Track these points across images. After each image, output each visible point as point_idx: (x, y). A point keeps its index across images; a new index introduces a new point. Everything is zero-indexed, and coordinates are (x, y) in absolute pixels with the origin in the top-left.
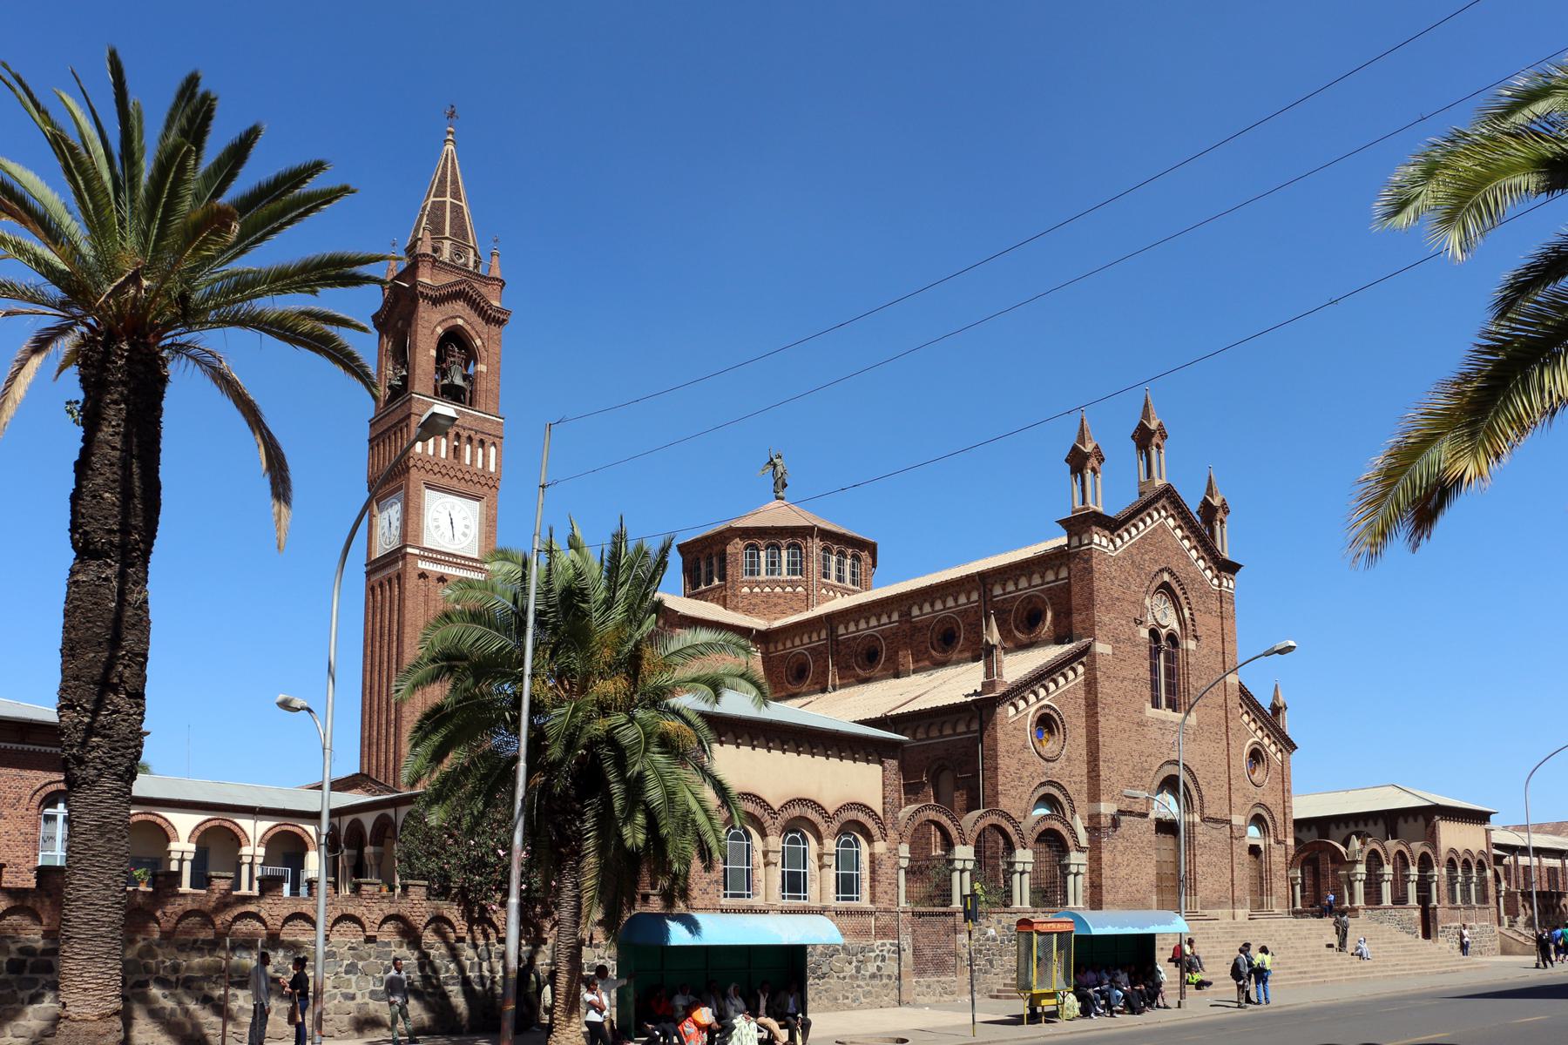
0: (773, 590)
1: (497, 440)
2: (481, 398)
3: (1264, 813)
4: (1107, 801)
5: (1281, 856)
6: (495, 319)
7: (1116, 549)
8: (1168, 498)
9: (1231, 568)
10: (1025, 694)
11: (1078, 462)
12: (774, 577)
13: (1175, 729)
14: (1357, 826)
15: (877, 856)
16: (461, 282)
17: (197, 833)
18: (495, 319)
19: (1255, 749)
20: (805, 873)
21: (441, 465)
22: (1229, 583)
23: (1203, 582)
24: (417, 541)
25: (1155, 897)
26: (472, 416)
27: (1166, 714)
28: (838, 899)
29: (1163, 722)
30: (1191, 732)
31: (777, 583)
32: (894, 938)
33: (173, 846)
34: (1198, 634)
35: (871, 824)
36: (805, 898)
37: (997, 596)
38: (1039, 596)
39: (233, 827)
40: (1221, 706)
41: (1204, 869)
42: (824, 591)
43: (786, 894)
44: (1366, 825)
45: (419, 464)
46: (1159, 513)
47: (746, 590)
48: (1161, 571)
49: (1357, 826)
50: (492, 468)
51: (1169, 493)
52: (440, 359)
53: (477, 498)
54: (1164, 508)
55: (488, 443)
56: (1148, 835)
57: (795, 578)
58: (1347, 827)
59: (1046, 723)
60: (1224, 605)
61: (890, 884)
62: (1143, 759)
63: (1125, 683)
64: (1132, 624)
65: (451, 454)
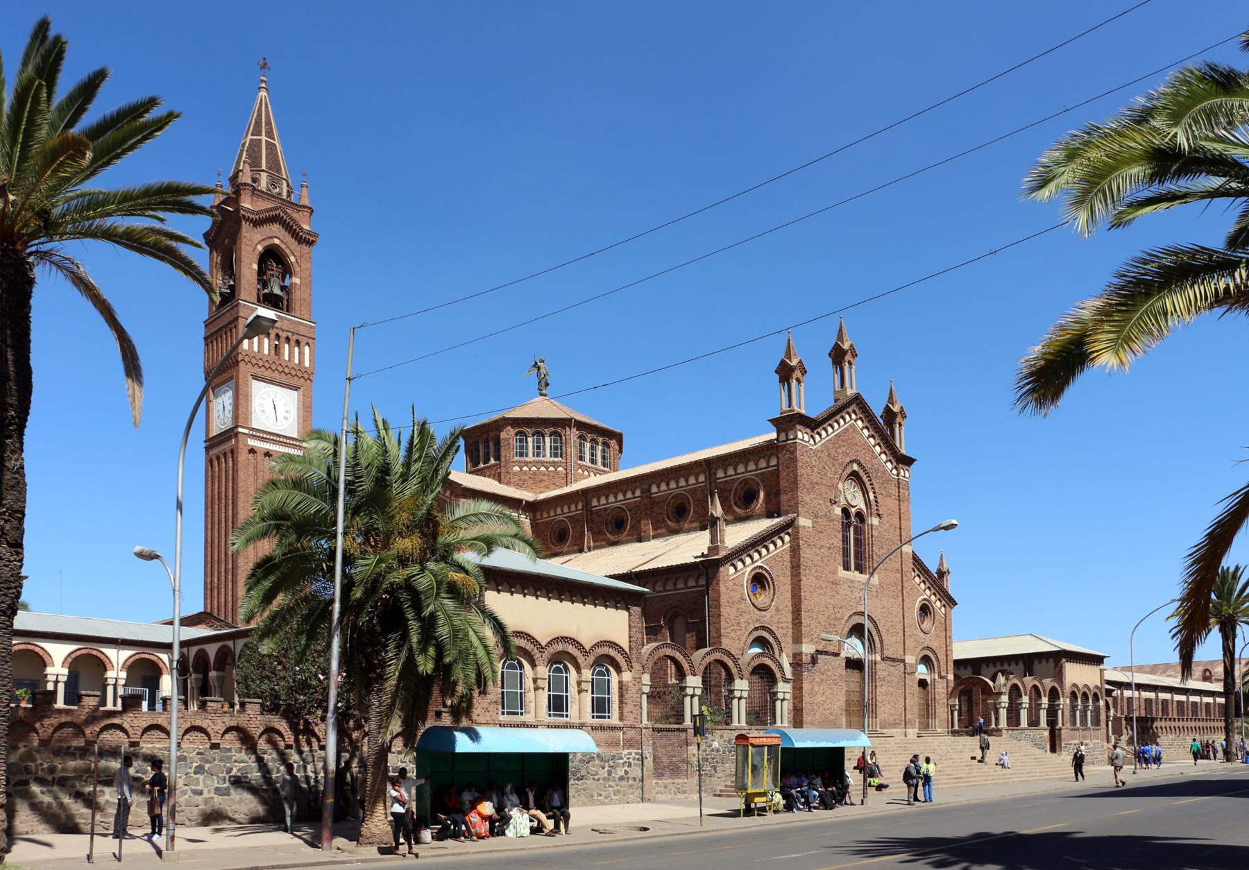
0: (538, 469)
1: (310, 341)
2: (296, 305)
3: (931, 655)
5: (943, 688)
6: (306, 240)
7: (815, 444)
8: (857, 404)
9: (907, 461)
10: (743, 557)
11: (785, 373)
12: (539, 459)
13: (861, 587)
14: (1002, 665)
15: (624, 683)
17: (70, 660)
18: (306, 240)
19: (924, 604)
20: (567, 696)
21: (264, 360)
22: (905, 473)
23: (884, 472)
24: (247, 422)
25: (844, 719)
26: (289, 320)
27: (854, 575)
28: (593, 717)
29: (852, 582)
30: (874, 590)
31: (542, 464)
32: (638, 749)
33: (49, 670)
34: (880, 513)
35: (619, 658)
36: (567, 716)
37: (720, 478)
38: (753, 480)
39: (99, 655)
40: (898, 570)
42: (580, 471)
43: (552, 713)
44: (1009, 665)
45: (247, 359)
46: (850, 416)
47: (516, 468)
48: (852, 462)
49: (1002, 665)
50: (307, 364)
51: (858, 400)
52: (261, 272)
53: (296, 388)
54: (854, 412)
55: (303, 341)
56: (839, 670)
57: (556, 459)
58: (995, 666)
59: (759, 580)
60: (901, 490)
61: (635, 706)
62: (836, 610)
63: (822, 550)
64: (828, 504)
65: (273, 352)
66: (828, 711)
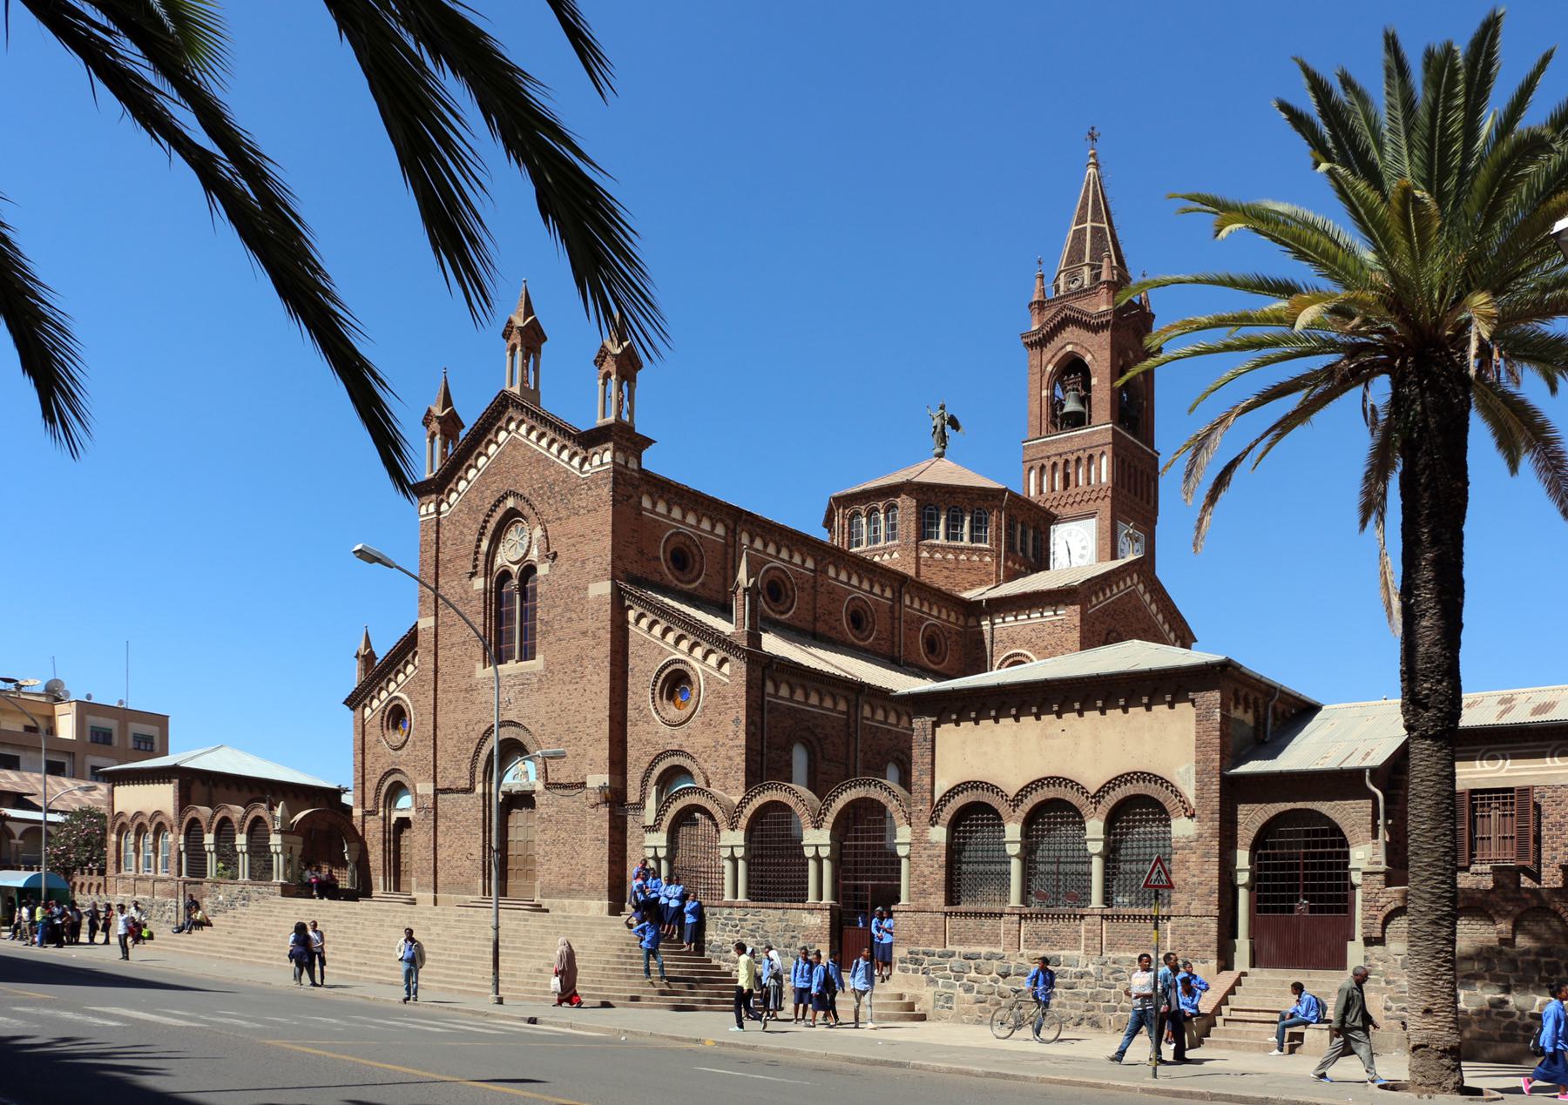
4: (423, 781)
16: (1061, 310)
41: (547, 848)
62: (470, 728)
66: (457, 870)
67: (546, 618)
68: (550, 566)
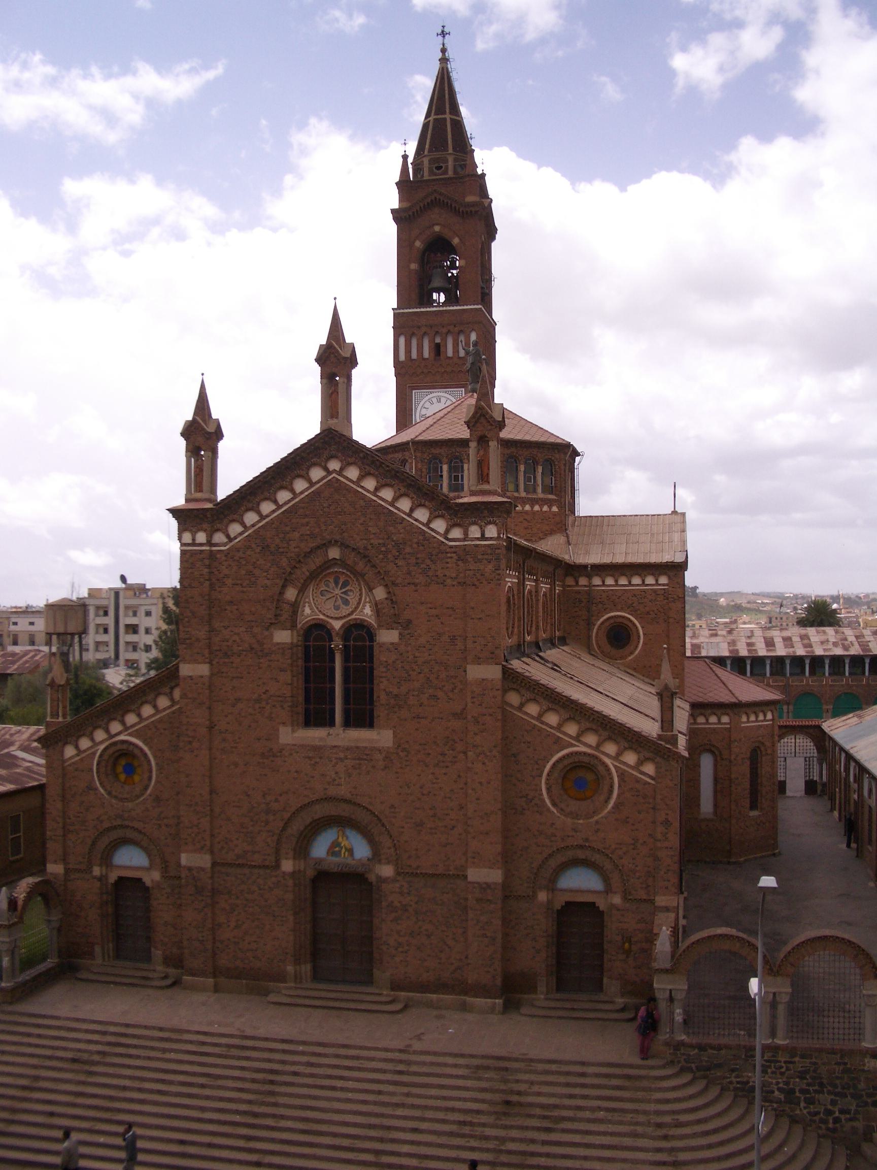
13: (342, 755)
67: (395, 691)
68: (400, 634)
